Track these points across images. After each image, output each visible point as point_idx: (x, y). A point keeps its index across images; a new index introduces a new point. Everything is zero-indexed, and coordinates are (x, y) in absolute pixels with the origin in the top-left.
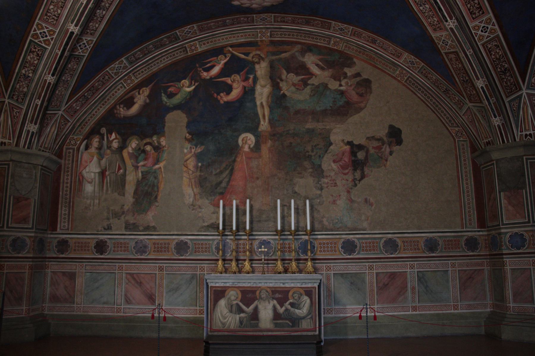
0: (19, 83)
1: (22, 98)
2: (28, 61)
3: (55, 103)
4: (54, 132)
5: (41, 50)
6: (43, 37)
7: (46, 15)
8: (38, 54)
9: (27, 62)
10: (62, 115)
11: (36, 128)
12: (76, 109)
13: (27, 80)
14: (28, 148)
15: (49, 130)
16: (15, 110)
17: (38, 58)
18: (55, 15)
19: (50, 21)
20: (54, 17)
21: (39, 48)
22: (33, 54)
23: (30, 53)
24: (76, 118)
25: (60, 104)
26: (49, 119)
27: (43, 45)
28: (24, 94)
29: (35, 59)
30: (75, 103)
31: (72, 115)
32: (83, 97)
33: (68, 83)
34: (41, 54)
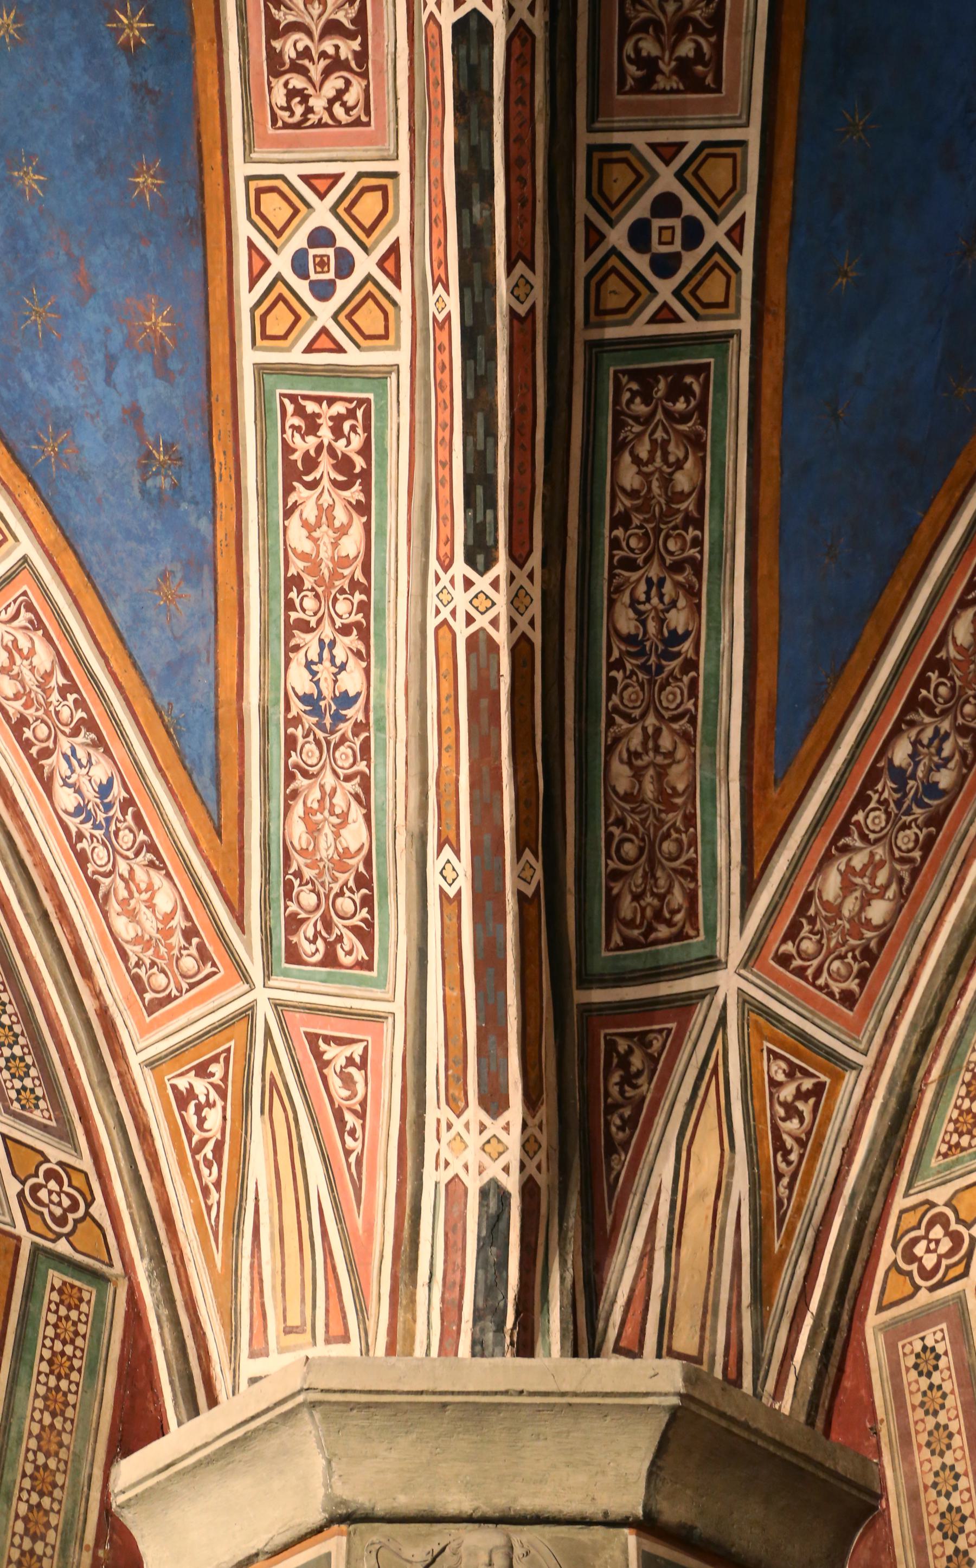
0: (294, 795)
1: (355, 930)
2: (297, 566)
3: (637, 897)
4: (721, 1189)
5: (351, 414)
6: (323, 291)
7: (274, 58)
8: (344, 464)
9: (295, 582)
10: (745, 1001)
11: (513, 1140)
12: (859, 923)
13: (343, 740)
14: (479, 1348)
15: (665, 1171)
16: (330, 1051)
17: (355, 494)
18: (333, 28)
19: (319, 103)
20: (328, 46)
21: (331, 401)
22: (312, 486)
23: (288, 490)
24: (894, 1025)
25: (692, 897)
26: (637, 1062)
27: (353, 357)
28: (363, 881)
29: (340, 516)
30: (827, 858)
31: (848, 999)
32: (886, 787)
33: (690, 665)
34: (365, 451)
